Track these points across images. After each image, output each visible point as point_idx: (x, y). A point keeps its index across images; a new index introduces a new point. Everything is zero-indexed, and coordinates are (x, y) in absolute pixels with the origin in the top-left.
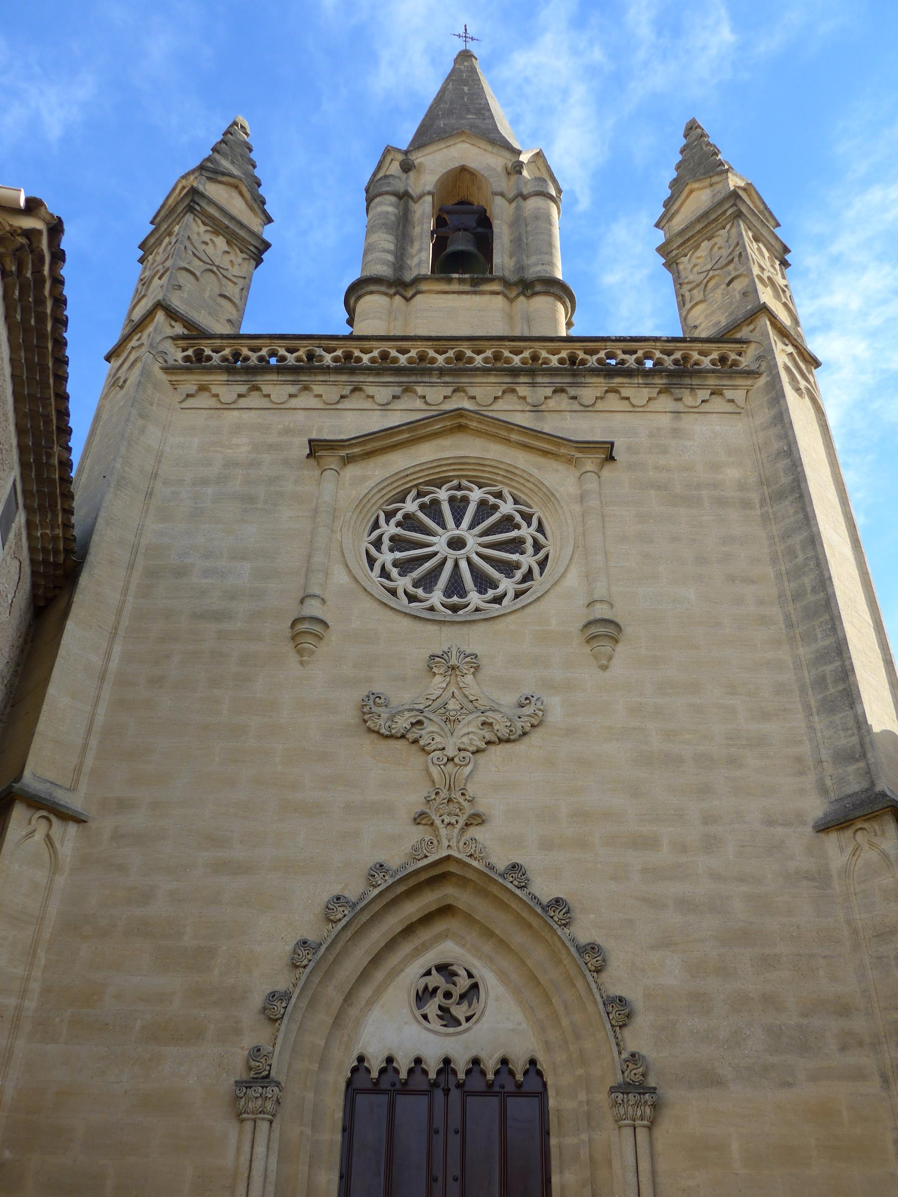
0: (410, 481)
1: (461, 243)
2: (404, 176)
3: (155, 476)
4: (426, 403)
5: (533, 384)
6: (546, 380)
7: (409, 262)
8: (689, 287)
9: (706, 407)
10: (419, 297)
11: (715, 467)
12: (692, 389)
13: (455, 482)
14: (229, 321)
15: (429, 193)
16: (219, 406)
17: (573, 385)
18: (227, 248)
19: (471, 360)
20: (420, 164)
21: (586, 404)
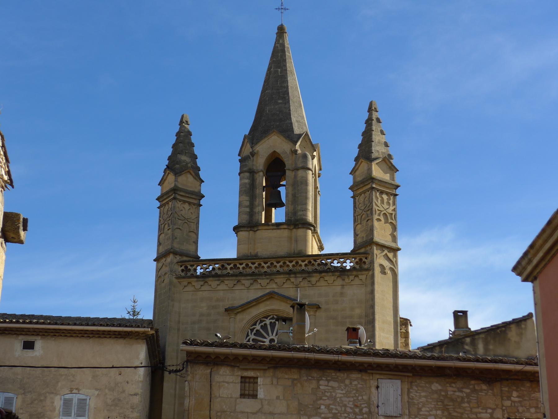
3: (179, 322)
5: (296, 277)
6: (300, 275)
7: (255, 210)
9: (353, 283)
12: (348, 276)
17: (309, 276)
20: (258, 151)
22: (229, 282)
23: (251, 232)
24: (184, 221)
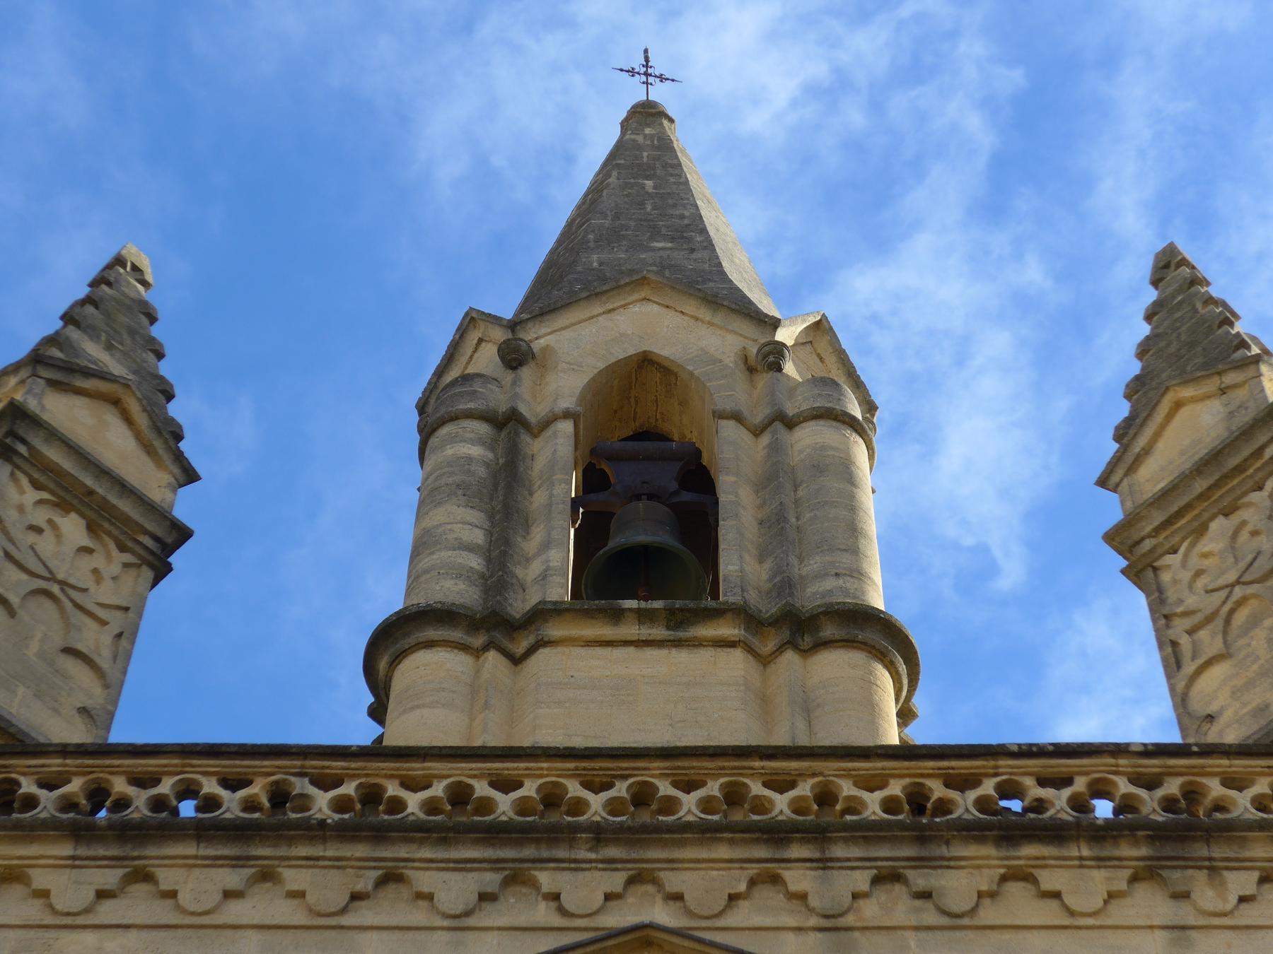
1: (642, 528)
2: (508, 377)
4: (562, 911)
5: (824, 863)
6: (855, 852)
7: (519, 571)
8: (1187, 623)
9: (1249, 915)
10: (543, 654)
12: (1213, 870)
14: (84, 711)
15: (567, 415)
16: (49, 920)
17: (921, 862)
18: (86, 541)
19: (670, 805)
20: (546, 349)
21: (955, 909)
22: (319, 880)
23: (492, 656)
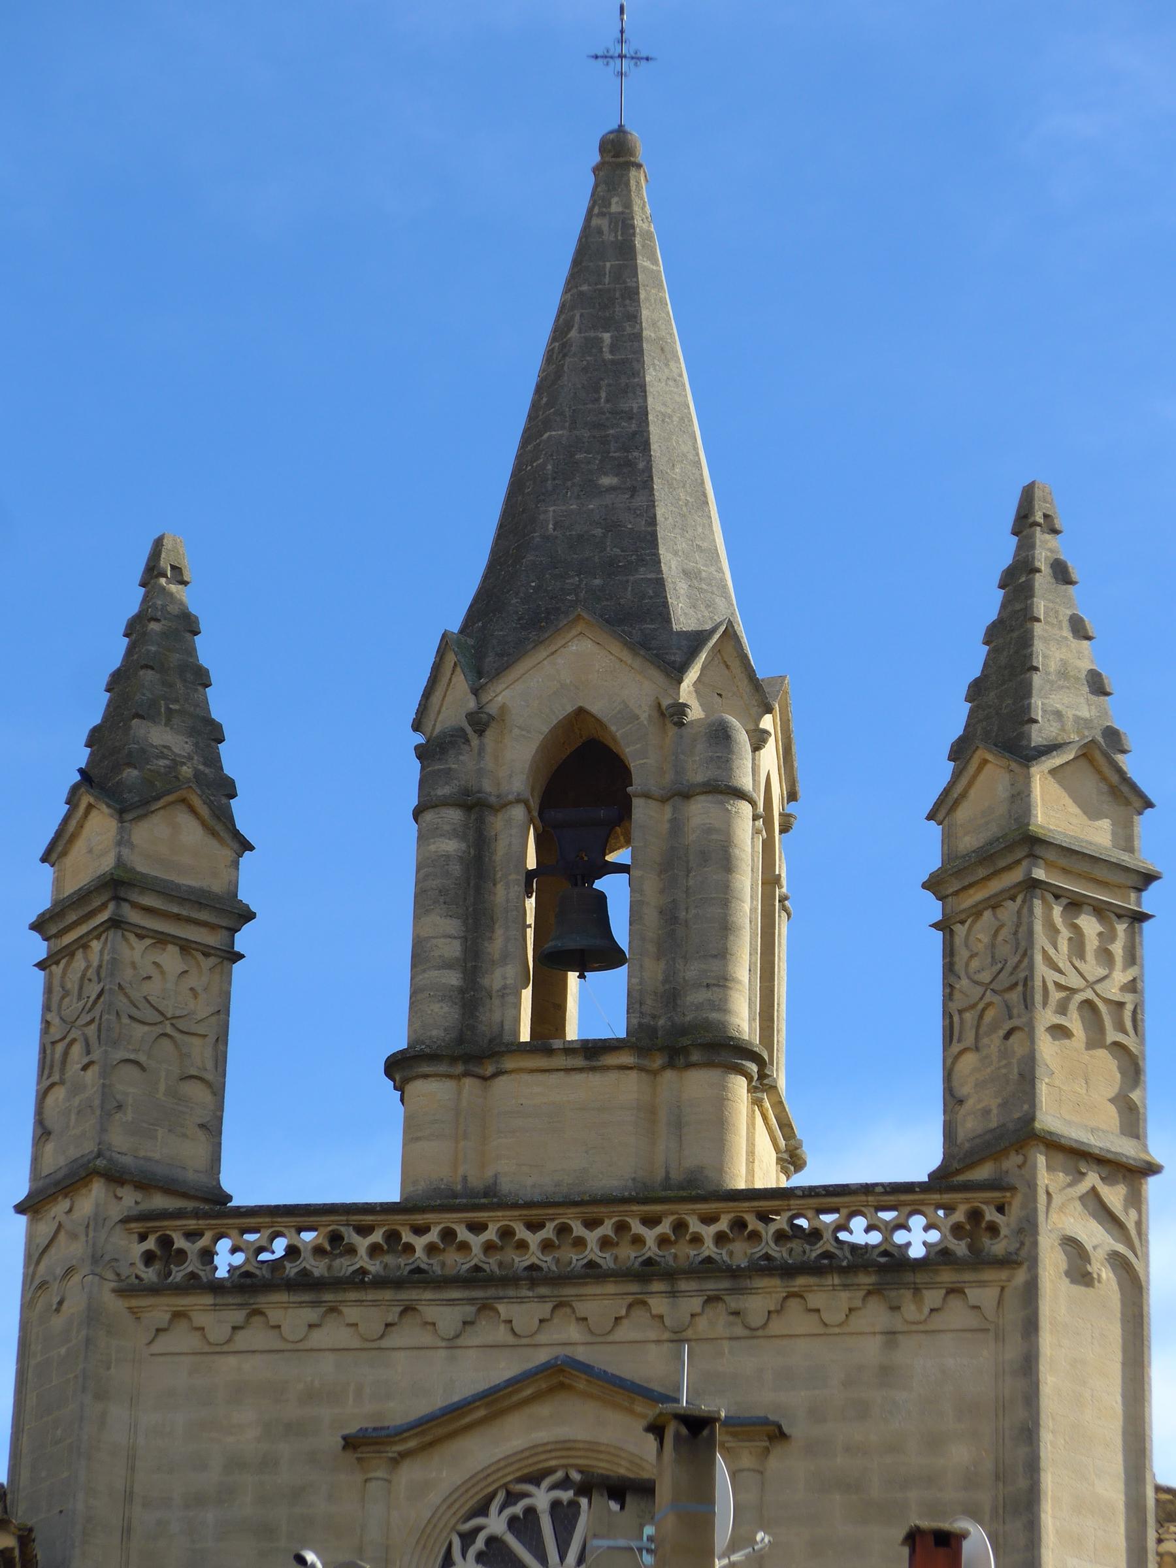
0: (494, 1482)
3: (129, 1497)
5: (673, 1294)
6: (692, 1285)
7: (486, 981)
9: (937, 1322)
11: (935, 1443)
12: (917, 1291)
13: (559, 1475)
16: (207, 1349)
17: (733, 1291)
20: (503, 708)
21: (753, 1325)
22: (363, 1314)
23: (468, 1082)
24: (158, 1030)
